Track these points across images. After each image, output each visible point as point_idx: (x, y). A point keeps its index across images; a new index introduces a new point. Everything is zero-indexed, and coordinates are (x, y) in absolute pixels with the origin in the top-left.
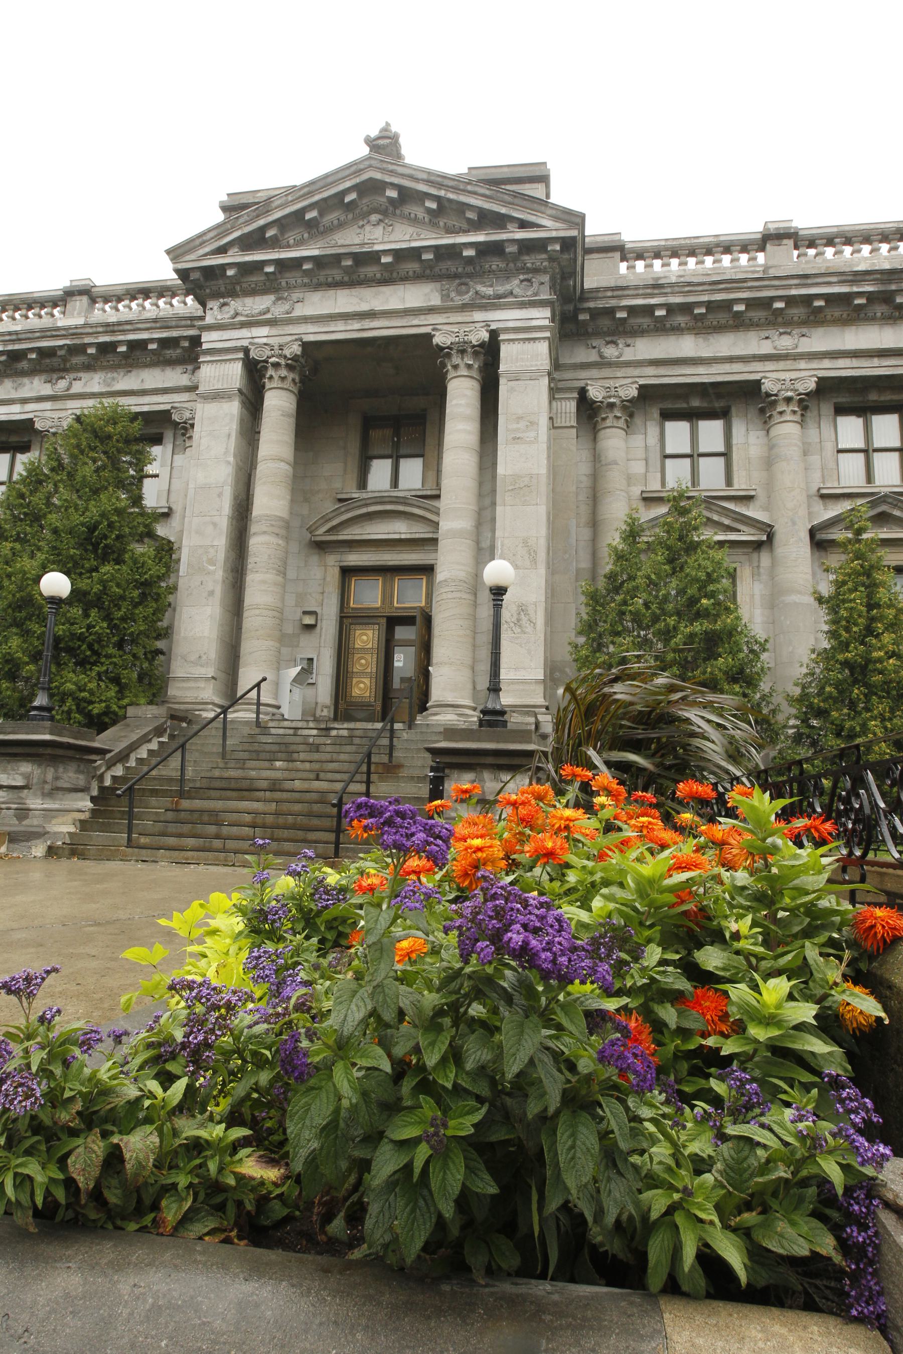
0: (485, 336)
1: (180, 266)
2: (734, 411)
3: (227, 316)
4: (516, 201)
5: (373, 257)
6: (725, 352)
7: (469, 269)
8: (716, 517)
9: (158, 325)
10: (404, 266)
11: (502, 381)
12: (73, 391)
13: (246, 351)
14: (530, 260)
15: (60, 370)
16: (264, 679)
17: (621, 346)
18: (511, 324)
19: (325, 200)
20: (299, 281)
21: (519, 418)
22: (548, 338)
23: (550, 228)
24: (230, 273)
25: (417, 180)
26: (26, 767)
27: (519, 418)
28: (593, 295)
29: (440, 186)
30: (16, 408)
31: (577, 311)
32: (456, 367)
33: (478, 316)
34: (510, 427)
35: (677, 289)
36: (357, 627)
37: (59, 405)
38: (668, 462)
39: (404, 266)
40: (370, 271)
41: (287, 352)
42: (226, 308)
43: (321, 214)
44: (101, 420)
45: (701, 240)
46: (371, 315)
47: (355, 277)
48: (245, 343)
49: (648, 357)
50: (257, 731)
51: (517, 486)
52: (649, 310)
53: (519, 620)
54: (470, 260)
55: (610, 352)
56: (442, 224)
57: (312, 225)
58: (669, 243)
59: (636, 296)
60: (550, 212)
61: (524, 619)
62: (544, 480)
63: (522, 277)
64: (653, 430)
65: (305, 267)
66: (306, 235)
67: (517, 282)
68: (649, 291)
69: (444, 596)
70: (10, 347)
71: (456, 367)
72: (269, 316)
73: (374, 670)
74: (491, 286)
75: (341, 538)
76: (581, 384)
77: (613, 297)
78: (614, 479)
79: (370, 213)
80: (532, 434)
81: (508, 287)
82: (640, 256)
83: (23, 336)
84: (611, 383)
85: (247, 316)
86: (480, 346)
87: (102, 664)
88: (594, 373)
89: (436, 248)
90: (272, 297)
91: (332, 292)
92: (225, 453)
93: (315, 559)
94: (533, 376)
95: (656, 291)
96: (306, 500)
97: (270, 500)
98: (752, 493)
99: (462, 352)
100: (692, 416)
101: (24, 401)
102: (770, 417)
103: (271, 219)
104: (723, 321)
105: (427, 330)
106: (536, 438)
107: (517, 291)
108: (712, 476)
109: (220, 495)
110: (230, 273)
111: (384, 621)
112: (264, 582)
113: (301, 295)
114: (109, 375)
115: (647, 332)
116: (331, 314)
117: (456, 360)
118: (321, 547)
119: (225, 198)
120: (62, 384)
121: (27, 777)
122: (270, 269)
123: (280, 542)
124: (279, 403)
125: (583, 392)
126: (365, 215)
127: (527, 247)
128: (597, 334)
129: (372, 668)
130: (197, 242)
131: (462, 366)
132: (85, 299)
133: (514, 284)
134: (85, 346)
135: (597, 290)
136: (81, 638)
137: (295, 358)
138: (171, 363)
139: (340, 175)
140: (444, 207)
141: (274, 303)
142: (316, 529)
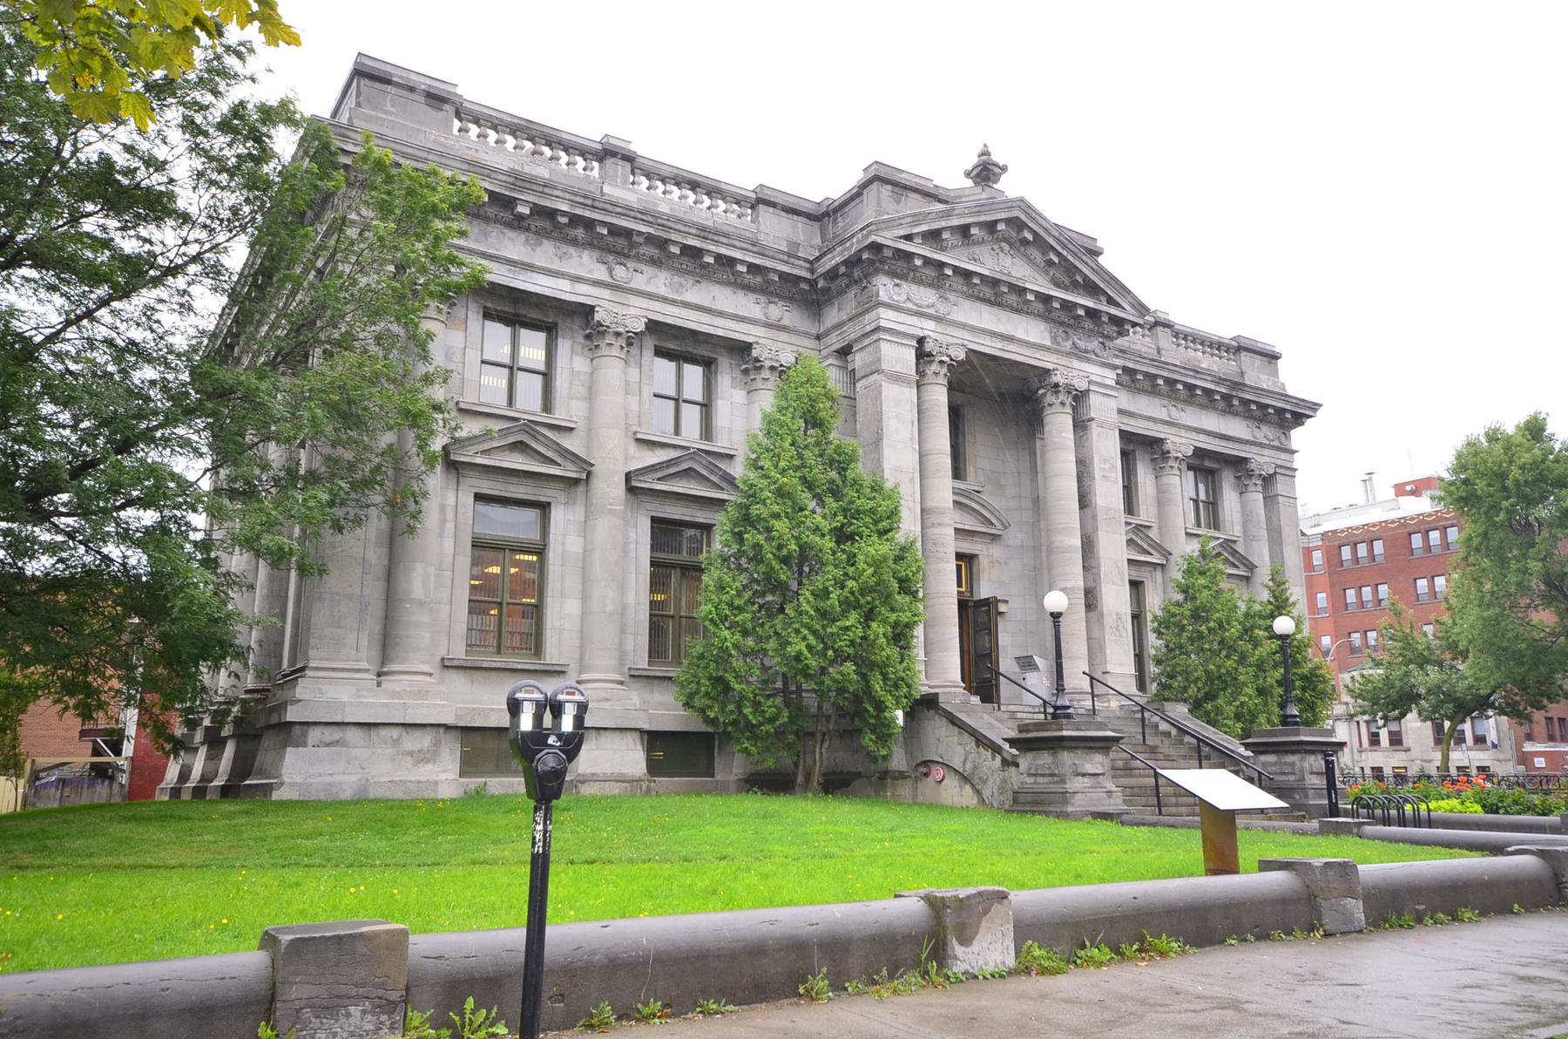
11: (1093, 424)
15: (618, 253)
29: (1064, 247)
30: (564, 285)
33: (1076, 364)
37: (619, 297)
40: (1013, 299)
41: (952, 352)
70: (579, 211)
71: (1063, 404)
83: (601, 205)
91: (978, 304)
101: (577, 279)
105: (1049, 366)
114: (676, 279)
117: (1062, 397)
120: (620, 272)
126: (998, 240)
132: (628, 166)
133: (1094, 344)
134: (667, 241)
138: (747, 288)
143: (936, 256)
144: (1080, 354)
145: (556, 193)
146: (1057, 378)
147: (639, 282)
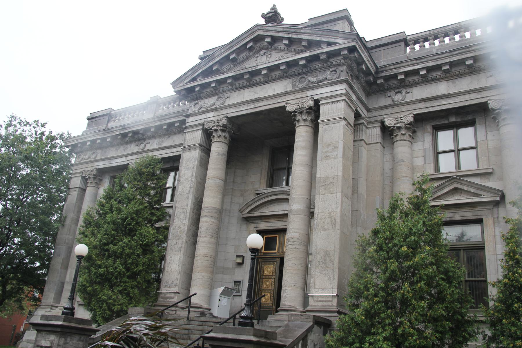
0: (311, 103)
1: (177, 90)
2: (477, 120)
3: (197, 109)
4: (324, 33)
5: (257, 72)
6: (465, 88)
7: (305, 70)
8: (465, 188)
9: (179, 114)
10: (273, 73)
12: (146, 149)
13: (203, 125)
14: (334, 61)
16: (195, 294)
17: (403, 94)
18: (326, 95)
19: (238, 48)
20: (227, 88)
21: (328, 145)
22: (345, 100)
23: (342, 43)
24: (197, 89)
25: (278, 32)
26: (53, 337)
27: (328, 145)
28: (384, 69)
30: (124, 159)
31: (376, 79)
32: (298, 121)
33: (310, 93)
34: (324, 151)
35: (430, 58)
36: (266, 263)
38: (441, 156)
39: (273, 73)
40: (258, 78)
42: (197, 105)
43: (238, 55)
44: (141, 166)
45: (450, 27)
46: (258, 100)
47: (252, 82)
48: (202, 121)
49: (419, 98)
50: (186, 322)
51: (327, 183)
52: (416, 72)
53: (325, 260)
54: (304, 66)
55: (398, 98)
56: (293, 50)
57: (234, 60)
58: (431, 32)
59: (408, 66)
60: (340, 35)
61: (328, 259)
62: (340, 179)
63: (331, 70)
64: (428, 139)
65: (228, 82)
66: (232, 66)
67: (328, 72)
68: (414, 62)
69: (288, 247)
70: (122, 132)
71: (298, 121)
72: (214, 107)
73: (273, 288)
74: (317, 76)
75: (256, 215)
76: (380, 118)
77: (395, 68)
78: (403, 171)
79: (260, 50)
80: (335, 153)
81: (324, 76)
82: (416, 42)
84: (399, 115)
85: (205, 108)
86: (309, 109)
87: (121, 286)
88: (389, 111)
89: (287, 63)
90: (216, 97)
91: (242, 91)
92: (192, 176)
93: (244, 226)
94: (336, 120)
95: (418, 62)
96: (242, 195)
97: (211, 200)
98: (491, 171)
99: (301, 113)
100: (455, 126)
101: (127, 155)
102: (498, 122)
103: (214, 62)
104: (462, 71)
105: (283, 104)
106: (337, 155)
107: (329, 77)
108: (469, 162)
109: (188, 198)
110: (197, 89)
111: (278, 260)
112: (204, 242)
113: (228, 95)
115: (418, 83)
116: (243, 102)
117: (298, 117)
118: (247, 220)
119: (202, 54)
120: (142, 146)
121: (52, 342)
122: (213, 85)
123: (213, 220)
124: (218, 149)
125: (383, 123)
127: (331, 55)
128: (389, 89)
129: (272, 287)
130: (184, 78)
131: (301, 120)
133: (328, 74)
135: (385, 66)
136: (112, 274)
137: (224, 126)
139: (244, 36)
140: (292, 41)
141: (217, 100)
142: (244, 210)
143: (204, 82)
144: (318, 85)
145: (115, 129)
146: (289, 108)
147: (148, 147)
